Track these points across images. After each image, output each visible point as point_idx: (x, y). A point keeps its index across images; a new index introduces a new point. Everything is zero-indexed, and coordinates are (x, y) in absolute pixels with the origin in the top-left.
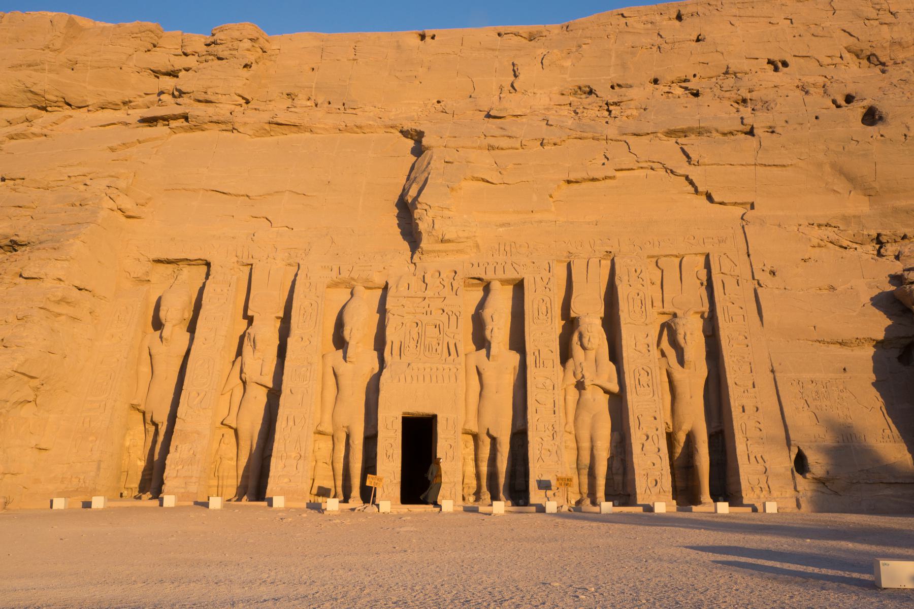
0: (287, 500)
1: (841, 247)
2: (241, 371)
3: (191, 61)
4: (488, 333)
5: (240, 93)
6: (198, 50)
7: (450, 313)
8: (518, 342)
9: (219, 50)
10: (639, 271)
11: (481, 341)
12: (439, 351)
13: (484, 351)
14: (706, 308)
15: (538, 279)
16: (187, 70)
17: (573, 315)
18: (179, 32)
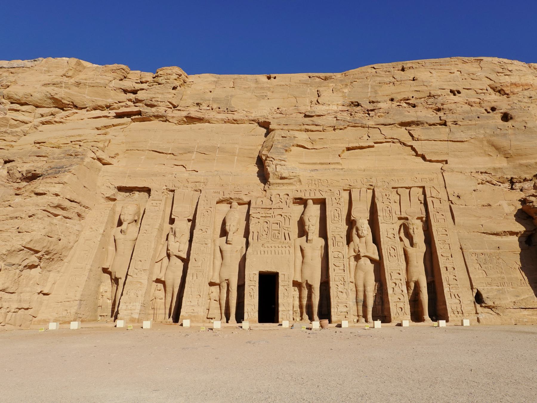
0: (192, 321)
1: (493, 184)
2: (168, 250)
3: (144, 86)
4: (306, 227)
5: (170, 101)
6: (148, 80)
7: (285, 217)
8: (323, 233)
9: (160, 80)
10: (388, 196)
11: (303, 232)
12: (279, 237)
13: (305, 237)
14: (424, 215)
15: (334, 199)
16: (143, 89)
17: (352, 218)
18: (139, 72)
